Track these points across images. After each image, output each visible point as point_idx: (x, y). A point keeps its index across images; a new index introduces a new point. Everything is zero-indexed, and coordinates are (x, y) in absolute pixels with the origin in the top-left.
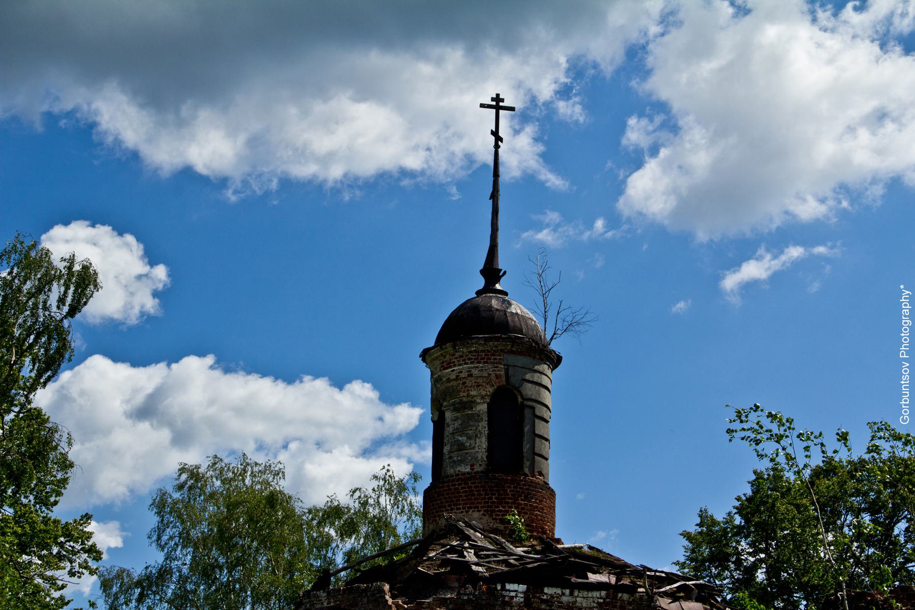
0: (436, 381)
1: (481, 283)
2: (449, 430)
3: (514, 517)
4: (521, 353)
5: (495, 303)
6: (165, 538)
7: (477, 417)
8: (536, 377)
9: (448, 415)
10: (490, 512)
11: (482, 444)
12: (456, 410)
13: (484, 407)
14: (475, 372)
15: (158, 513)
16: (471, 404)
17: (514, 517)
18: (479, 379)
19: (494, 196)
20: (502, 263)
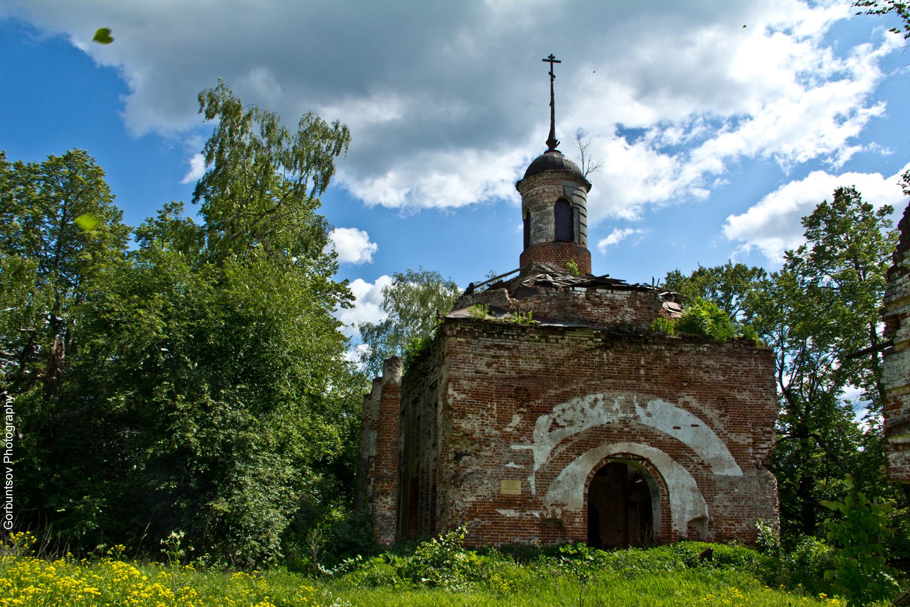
1: (546, 147)
2: (532, 222)
3: (573, 265)
4: (571, 180)
5: (555, 155)
6: (388, 307)
7: (549, 213)
8: (579, 193)
9: (532, 214)
10: (557, 262)
11: (552, 227)
12: (537, 210)
13: (551, 208)
14: (547, 190)
16: (545, 206)
17: (573, 265)
18: (549, 192)
19: (552, 104)
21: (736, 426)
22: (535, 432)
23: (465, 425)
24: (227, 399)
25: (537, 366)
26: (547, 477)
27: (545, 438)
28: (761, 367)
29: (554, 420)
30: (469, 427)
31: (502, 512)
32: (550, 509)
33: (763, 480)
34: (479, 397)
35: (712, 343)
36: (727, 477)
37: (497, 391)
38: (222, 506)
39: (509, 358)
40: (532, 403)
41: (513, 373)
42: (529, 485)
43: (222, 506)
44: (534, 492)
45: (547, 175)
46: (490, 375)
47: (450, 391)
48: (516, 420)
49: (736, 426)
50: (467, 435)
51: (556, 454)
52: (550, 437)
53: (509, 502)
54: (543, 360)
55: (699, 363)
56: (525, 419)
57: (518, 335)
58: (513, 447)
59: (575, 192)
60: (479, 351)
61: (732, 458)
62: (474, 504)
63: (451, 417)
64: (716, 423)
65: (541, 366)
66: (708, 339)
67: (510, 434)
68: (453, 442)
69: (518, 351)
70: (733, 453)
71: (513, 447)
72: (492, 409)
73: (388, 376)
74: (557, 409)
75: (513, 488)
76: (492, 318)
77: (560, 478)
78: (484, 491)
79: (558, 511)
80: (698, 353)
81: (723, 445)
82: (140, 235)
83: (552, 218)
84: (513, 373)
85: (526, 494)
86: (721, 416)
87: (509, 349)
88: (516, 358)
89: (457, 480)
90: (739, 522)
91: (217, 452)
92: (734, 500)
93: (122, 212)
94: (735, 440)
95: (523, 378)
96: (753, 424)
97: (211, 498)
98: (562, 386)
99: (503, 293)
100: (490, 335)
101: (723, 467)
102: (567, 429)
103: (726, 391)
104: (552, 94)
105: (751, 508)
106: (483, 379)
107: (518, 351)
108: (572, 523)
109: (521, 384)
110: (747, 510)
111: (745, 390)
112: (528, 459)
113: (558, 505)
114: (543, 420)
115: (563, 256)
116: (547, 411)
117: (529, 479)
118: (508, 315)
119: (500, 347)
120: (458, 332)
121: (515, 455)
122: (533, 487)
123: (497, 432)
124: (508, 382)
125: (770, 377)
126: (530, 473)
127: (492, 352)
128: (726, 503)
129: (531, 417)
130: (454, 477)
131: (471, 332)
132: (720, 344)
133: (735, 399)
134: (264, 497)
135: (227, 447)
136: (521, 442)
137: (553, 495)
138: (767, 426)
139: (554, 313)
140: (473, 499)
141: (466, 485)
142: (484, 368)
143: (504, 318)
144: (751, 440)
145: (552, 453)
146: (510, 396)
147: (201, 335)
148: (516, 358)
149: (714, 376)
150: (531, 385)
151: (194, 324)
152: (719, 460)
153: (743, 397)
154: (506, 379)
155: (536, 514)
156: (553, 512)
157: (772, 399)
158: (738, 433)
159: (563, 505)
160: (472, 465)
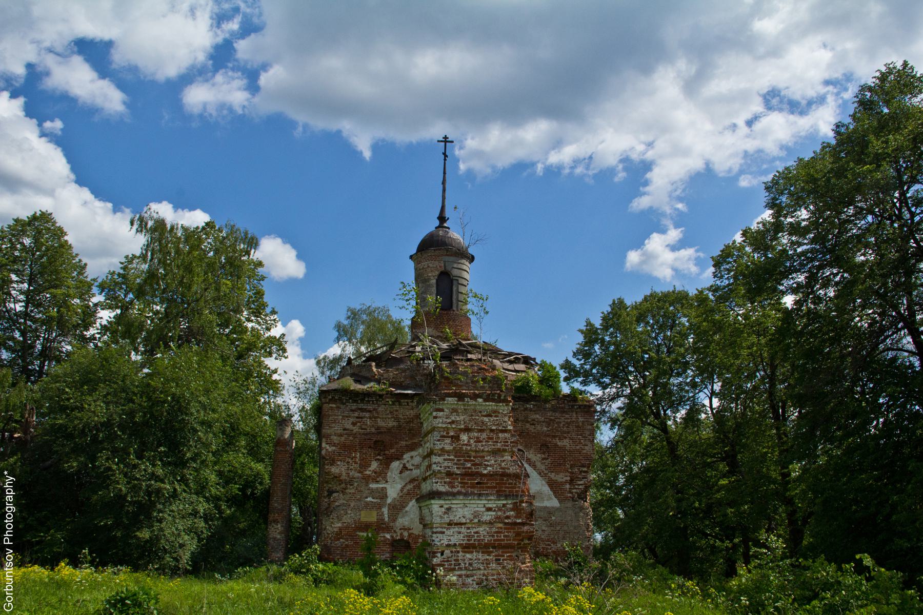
0: (416, 269)
1: (437, 223)
5: (441, 233)
7: (429, 286)
10: (436, 328)
13: (434, 281)
15: (338, 331)
16: (428, 280)
19: (444, 183)
20: (447, 214)
21: (556, 467)
22: (389, 474)
23: (334, 470)
24: (148, 460)
25: (392, 423)
26: (397, 508)
27: (397, 478)
28: (581, 419)
29: (404, 465)
30: (337, 471)
31: (361, 534)
33: (577, 510)
34: (346, 449)
35: (539, 401)
36: (546, 508)
37: (360, 444)
38: (145, 534)
39: (370, 418)
40: (387, 452)
42: (383, 514)
43: (145, 534)
44: (386, 519)
45: (431, 252)
46: (355, 431)
47: (324, 445)
48: (374, 465)
49: (556, 467)
50: (337, 478)
51: (405, 490)
52: (401, 478)
53: (366, 527)
54: (397, 419)
55: (526, 417)
56: (381, 464)
59: (455, 266)
61: (551, 493)
62: (340, 529)
63: (324, 464)
64: (538, 464)
65: (395, 424)
66: (536, 398)
67: (369, 476)
68: (327, 482)
69: (378, 413)
70: (551, 489)
72: (355, 457)
73: (279, 434)
74: (406, 456)
75: (372, 517)
76: (359, 387)
77: (407, 509)
78: (349, 518)
79: (406, 534)
80: (526, 409)
81: (544, 482)
82: (102, 287)
83: (434, 289)
84: (373, 430)
85: (381, 521)
86: (543, 459)
87: (370, 411)
88: (376, 418)
89: (328, 511)
90: (555, 543)
91: (142, 497)
93: (86, 264)
94: (554, 478)
95: (381, 433)
96: (572, 466)
97: (138, 529)
99: (371, 366)
101: (542, 500)
103: (548, 439)
104: (445, 173)
105: (566, 532)
106: (349, 435)
107: (378, 413)
108: (416, 543)
109: (379, 438)
110: (562, 533)
111: (565, 438)
112: (383, 495)
113: (405, 529)
114: (396, 465)
115: (442, 323)
116: (399, 457)
118: (372, 384)
119: (362, 410)
120: (330, 400)
121: (372, 492)
123: (359, 475)
124: (368, 437)
125: (590, 427)
126: (384, 505)
127: (356, 414)
128: (544, 528)
129: (386, 463)
130: (326, 509)
131: (340, 399)
132: (546, 401)
133: (556, 445)
134: (180, 526)
136: (377, 482)
137: (402, 521)
138: (583, 466)
139: (408, 382)
140: (340, 525)
141: (334, 515)
143: (372, 386)
144: (568, 478)
145: (402, 490)
146: (370, 447)
147: (131, 414)
148: (376, 418)
149: (539, 427)
151: (126, 408)
152: (540, 493)
154: (366, 434)
155: (388, 536)
156: (401, 534)
157: (590, 445)
158: (557, 473)
160: (339, 499)
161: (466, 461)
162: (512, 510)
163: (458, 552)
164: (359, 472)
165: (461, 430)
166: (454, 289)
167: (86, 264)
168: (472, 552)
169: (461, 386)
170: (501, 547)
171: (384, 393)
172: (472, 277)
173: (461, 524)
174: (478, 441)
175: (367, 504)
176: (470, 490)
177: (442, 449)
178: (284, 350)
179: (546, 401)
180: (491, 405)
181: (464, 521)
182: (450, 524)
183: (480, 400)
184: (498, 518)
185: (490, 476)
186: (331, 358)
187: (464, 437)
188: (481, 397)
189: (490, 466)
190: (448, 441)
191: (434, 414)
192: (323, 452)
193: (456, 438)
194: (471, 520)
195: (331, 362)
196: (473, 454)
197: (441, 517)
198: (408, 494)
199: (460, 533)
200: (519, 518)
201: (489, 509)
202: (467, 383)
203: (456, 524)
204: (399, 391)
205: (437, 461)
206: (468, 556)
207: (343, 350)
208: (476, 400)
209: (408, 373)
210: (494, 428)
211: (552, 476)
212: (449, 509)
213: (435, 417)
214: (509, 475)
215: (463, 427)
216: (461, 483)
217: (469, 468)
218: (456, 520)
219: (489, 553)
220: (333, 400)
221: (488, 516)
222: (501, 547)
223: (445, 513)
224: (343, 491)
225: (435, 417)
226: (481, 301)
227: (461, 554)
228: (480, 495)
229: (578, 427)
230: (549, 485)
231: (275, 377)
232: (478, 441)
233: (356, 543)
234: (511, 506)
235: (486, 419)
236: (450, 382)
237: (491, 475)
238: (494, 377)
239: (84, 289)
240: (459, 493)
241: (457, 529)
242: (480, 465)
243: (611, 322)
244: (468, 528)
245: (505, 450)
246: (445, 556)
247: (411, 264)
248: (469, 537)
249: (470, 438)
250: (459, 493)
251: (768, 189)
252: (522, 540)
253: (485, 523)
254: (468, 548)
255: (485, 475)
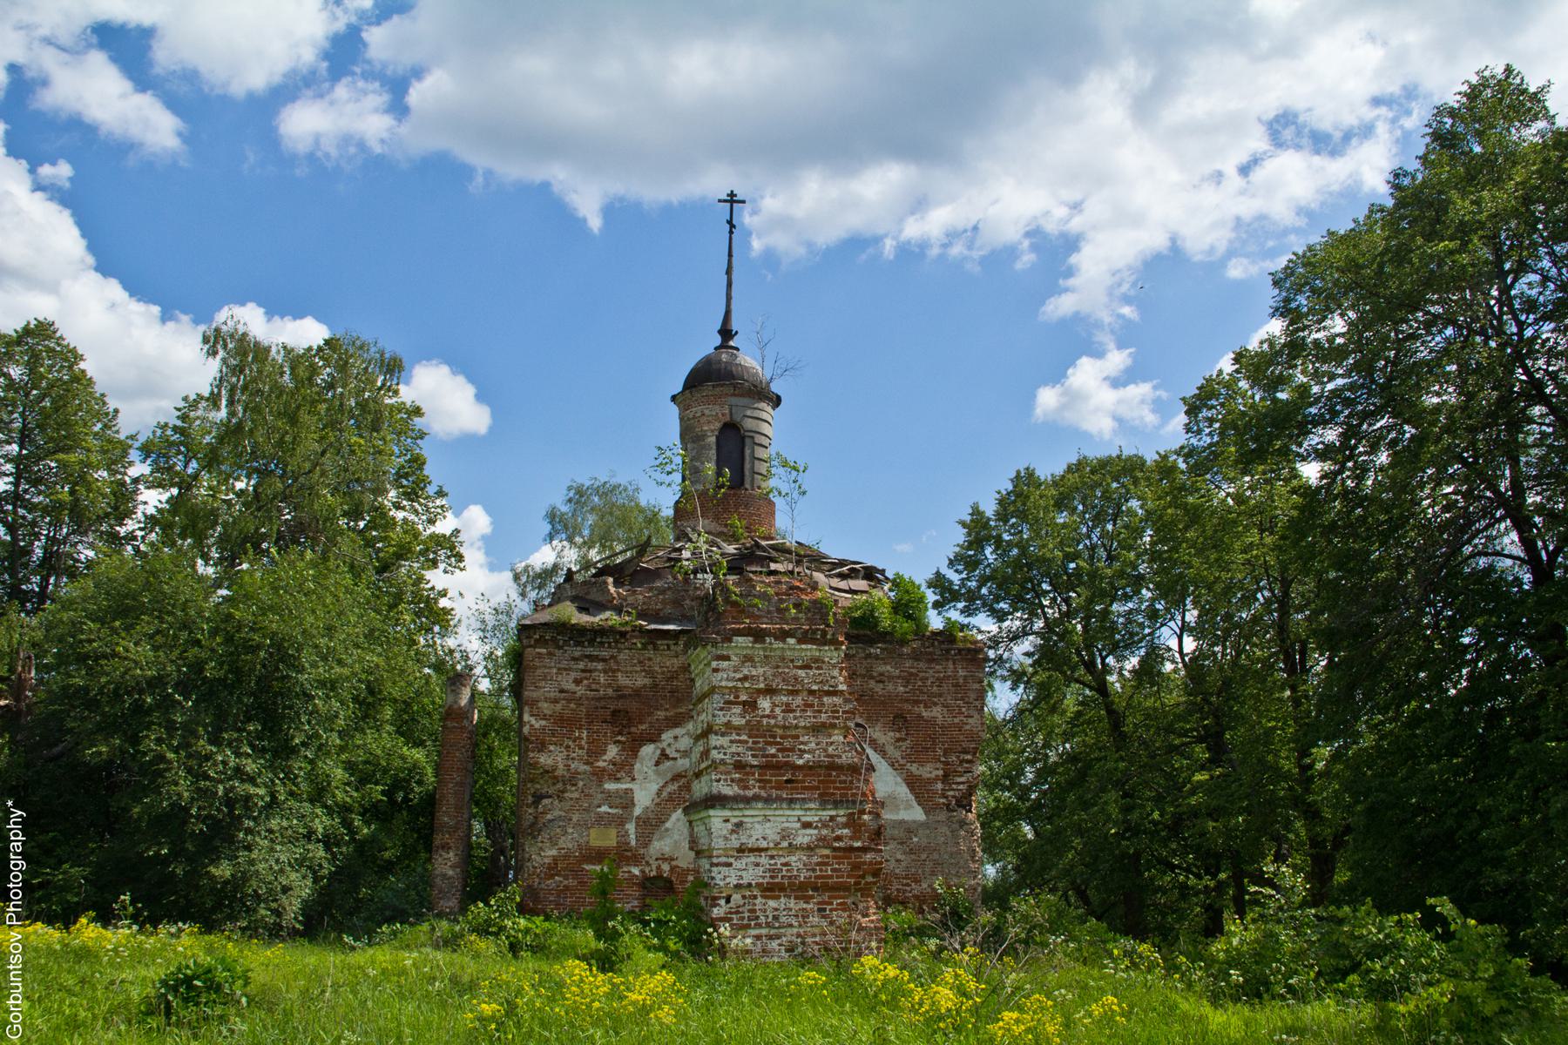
0: (681, 419)
1: (718, 340)
4: (742, 395)
5: (724, 357)
8: (757, 414)
10: (717, 518)
13: (713, 439)
19: (729, 272)
21: (919, 753)
22: (637, 766)
23: (544, 760)
24: (229, 745)
25: (641, 681)
26: (651, 824)
27: (650, 773)
28: (961, 673)
29: (663, 750)
30: (550, 762)
32: (654, 865)
33: (956, 826)
34: (565, 723)
35: (891, 642)
36: (902, 822)
37: (588, 716)
38: (223, 870)
39: (605, 672)
40: (633, 729)
41: (610, 692)
43: (223, 870)
44: (633, 843)
45: (708, 389)
47: (526, 717)
48: (612, 751)
49: (919, 753)
50: (548, 772)
51: (665, 794)
52: (657, 773)
53: (599, 855)
54: (650, 673)
55: (870, 669)
56: (623, 750)
57: (616, 642)
58: (607, 786)
59: (749, 413)
60: (564, 664)
62: (555, 859)
63: (527, 750)
64: (890, 749)
65: (647, 681)
66: (885, 636)
67: (604, 770)
68: (532, 781)
69: (617, 662)
71: (607, 786)
73: (451, 699)
74: (667, 736)
75: (609, 839)
77: (668, 825)
78: (569, 841)
79: (666, 867)
80: (869, 656)
81: (899, 780)
82: (146, 450)
83: (713, 453)
84: (610, 692)
86: (898, 740)
87: (604, 660)
88: (614, 671)
89: (535, 830)
90: (917, 881)
92: (911, 851)
93: (116, 411)
97: (212, 862)
98: (675, 707)
99: (606, 583)
100: (578, 644)
101: (897, 808)
102: (680, 762)
103: (907, 706)
104: (730, 255)
105: (936, 863)
106: (569, 701)
107: (617, 662)
108: (683, 882)
109: (620, 705)
111: (935, 704)
112: (627, 801)
114: (648, 750)
115: (726, 510)
116: (653, 738)
117: (628, 826)
118: (608, 614)
119: (591, 658)
121: (609, 797)
122: (633, 836)
123: (587, 768)
124: (603, 703)
125: (977, 686)
127: (581, 665)
128: (899, 856)
130: (532, 825)
131: (554, 640)
132: (903, 642)
133: (920, 717)
135: (230, 802)
136: (618, 780)
137: (660, 846)
138: (966, 752)
140: (554, 852)
141: (545, 835)
142: (572, 687)
143: (608, 618)
144: (941, 773)
147: (198, 667)
148: (614, 671)
149: (890, 687)
150: (633, 706)
153: (934, 714)
155: (636, 871)
156: (659, 868)
157: (977, 716)
158: (921, 763)
159: (672, 859)
160: (553, 810)
161: (767, 743)
162: (845, 826)
163: (755, 897)
164: (587, 763)
165: (759, 691)
166: (747, 452)
167: (116, 411)
168: (778, 898)
169: (759, 617)
170: (827, 888)
171: (629, 629)
172: (777, 432)
173: (760, 850)
174: (788, 709)
175: (600, 817)
176: (774, 793)
177: (728, 724)
178: (460, 558)
179: (903, 642)
180: (810, 650)
181: (764, 844)
182: (741, 850)
183: (792, 641)
184: (823, 841)
185: (809, 768)
186: (538, 570)
187: (765, 704)
188: (792, 636)
189: (809, 752)
190: (737, 710)
191: (714, 664)
192: (526, 730)
193: (751, 705)
194: (777, 844)
195: (538, 576)
196: (780, 732)
197: (726, 838)
198: (670, 799)
199: (757, 865)
200: (858, 839)
201: (807, 825)
202: (769, 612)
203: (752, 850)
204: (653, 627)
205: (718, 743)
206: (772, 903)
207: (559, 556)
208: (784, 641)
209: (669, 595)
210: (815, 687)
211: (914, 768)
212: (739, 825)
213: (716, 670)
214: (839, 768)
215: (762, 686)
216: (760, 781)
217: (773, 756)
218: (751, 843)
219: (807, 899)
220: (541, 642)
221: (805, 837)
222: (827, 888)
223: (733, 831)
224: (560, 796)
225: (716, 670)
226: (794, 473)
227: (759, 900)
228: (791, 801)
229: (957, 685)
230: (908, 784)
231: (443, 603)
232: (788, 709)
233: (582, 883)
234: (844, 820)
235: (802, 673)
236: (739, 610)
237: (811, 768)
238: (815, 602)
239: (116, 454)
240: (756, 798)
241: (753, 859)
242: (792, 750)
243: (1012, 508)
244: (772, 857)
245: (833, 726)
246: (732, 904)
247: (674, 410)
248: (773, 872)
249: (774, 705)
250: (756, 798)
251: (1276, 283)
252: (863, 877)
253: (801, 848)
254: (771, 890)
255: (800, 768)
